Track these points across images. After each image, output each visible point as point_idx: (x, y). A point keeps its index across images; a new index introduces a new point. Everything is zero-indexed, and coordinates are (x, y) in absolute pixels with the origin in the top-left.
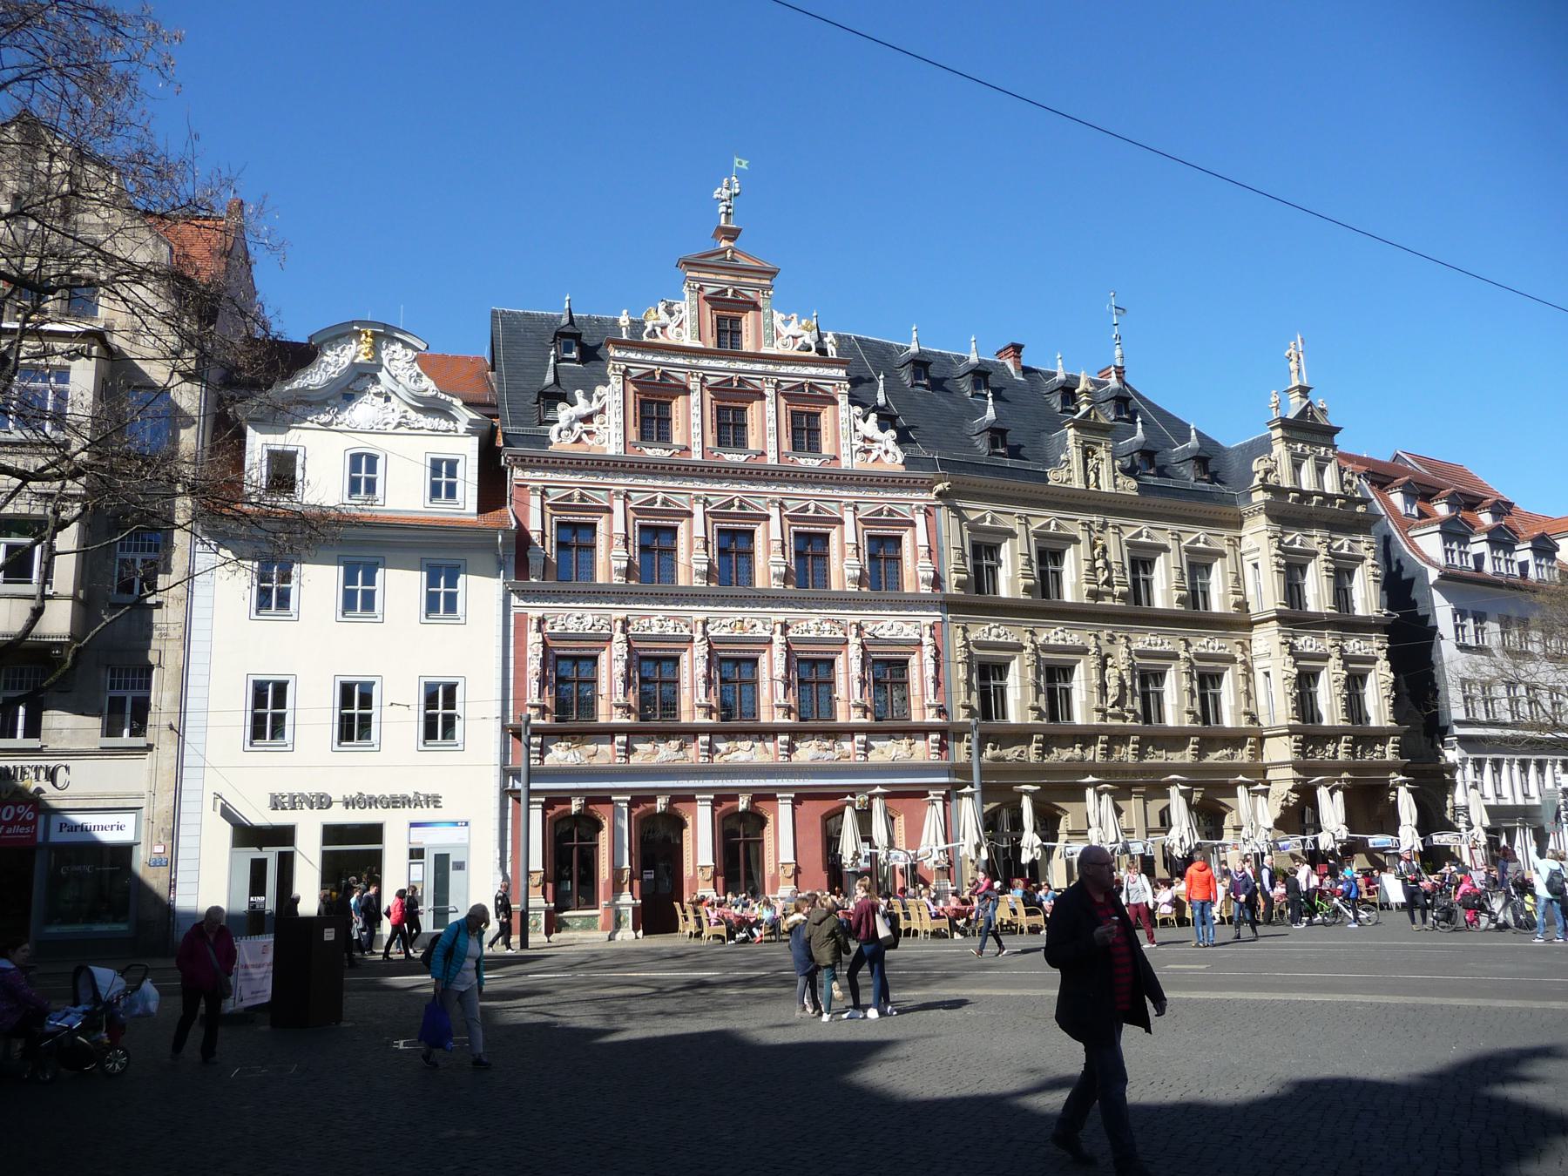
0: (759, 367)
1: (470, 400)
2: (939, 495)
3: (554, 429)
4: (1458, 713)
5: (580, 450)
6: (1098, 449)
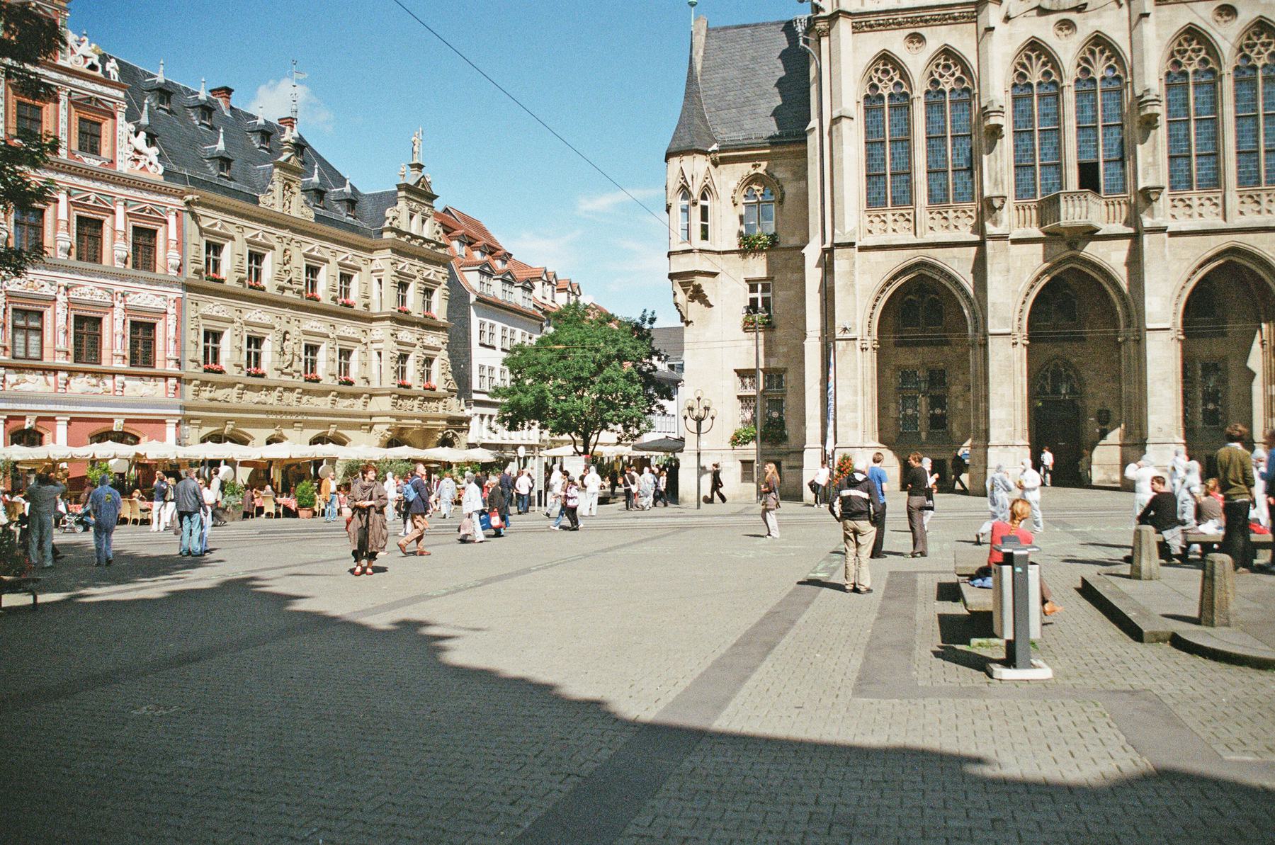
2: (188, 203)
4: (475, 386)
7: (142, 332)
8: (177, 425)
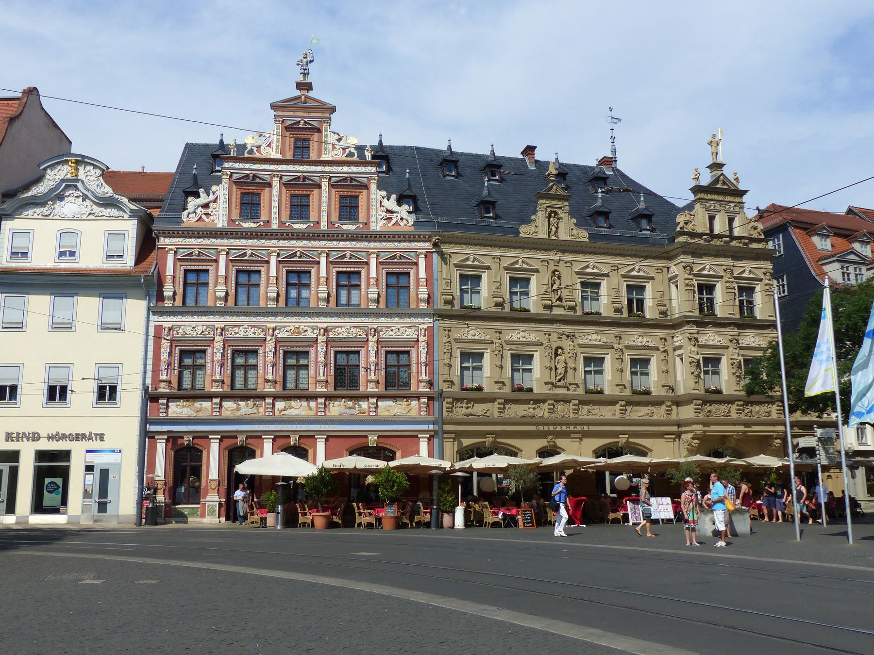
0: (319, 168)
1: (131, 197)
3: (186, 212)
5: (200, 225)
6: (559, 211)
7: (397, 359)
8: (429, 439)
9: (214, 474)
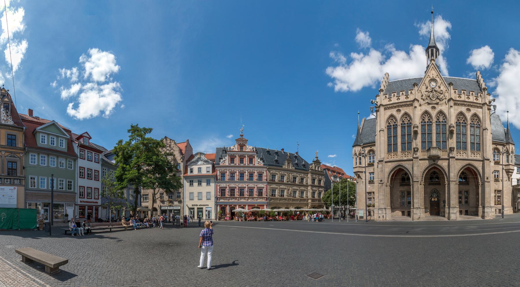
9: (228, 212)
